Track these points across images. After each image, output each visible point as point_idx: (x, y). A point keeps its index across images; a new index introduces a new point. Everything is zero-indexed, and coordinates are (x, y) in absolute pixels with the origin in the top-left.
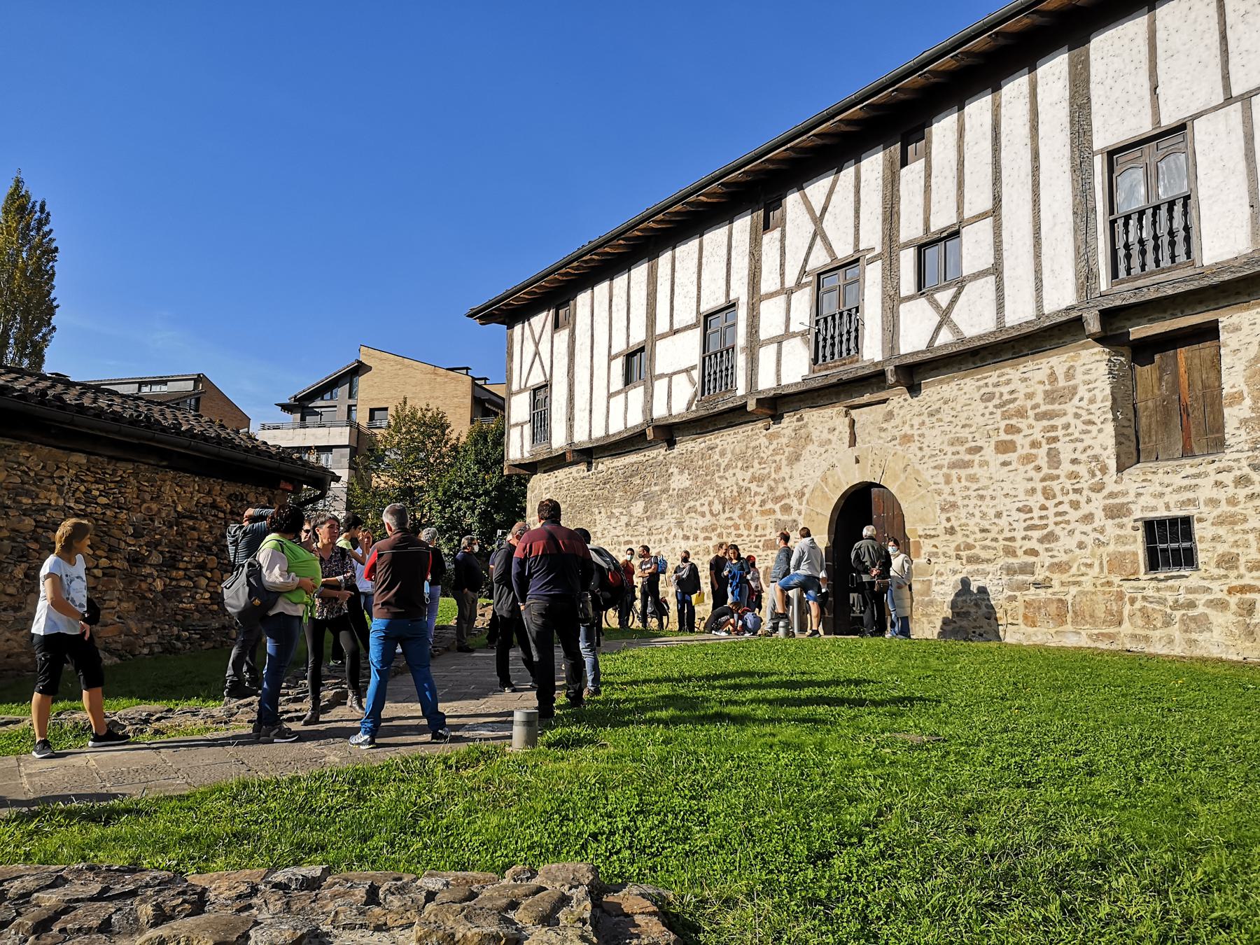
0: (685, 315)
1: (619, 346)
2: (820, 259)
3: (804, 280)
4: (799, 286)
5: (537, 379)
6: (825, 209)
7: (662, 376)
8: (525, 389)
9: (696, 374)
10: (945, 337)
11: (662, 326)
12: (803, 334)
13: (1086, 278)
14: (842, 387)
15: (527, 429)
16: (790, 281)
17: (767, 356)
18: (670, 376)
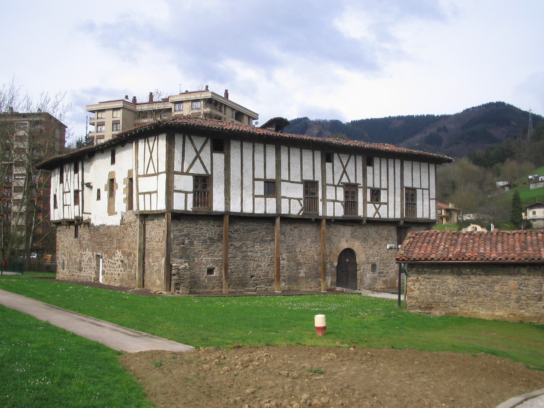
0: (295, 176)
1: (260, 174)
2: (345, 180)
3: (340, 184)
4: (338, 186)
5: (198, 169)
6: (346, 165)
7: (285, 197)
8: (187, 174)
9: (302, 202)
10: (377, 216)
11: (284, 175)
12: (341, 202)
13: (402, 214)
14: (351, 221)
15: (190, 197)
16: (336, 183)
17: (329, 205)
18: (290, 199)
